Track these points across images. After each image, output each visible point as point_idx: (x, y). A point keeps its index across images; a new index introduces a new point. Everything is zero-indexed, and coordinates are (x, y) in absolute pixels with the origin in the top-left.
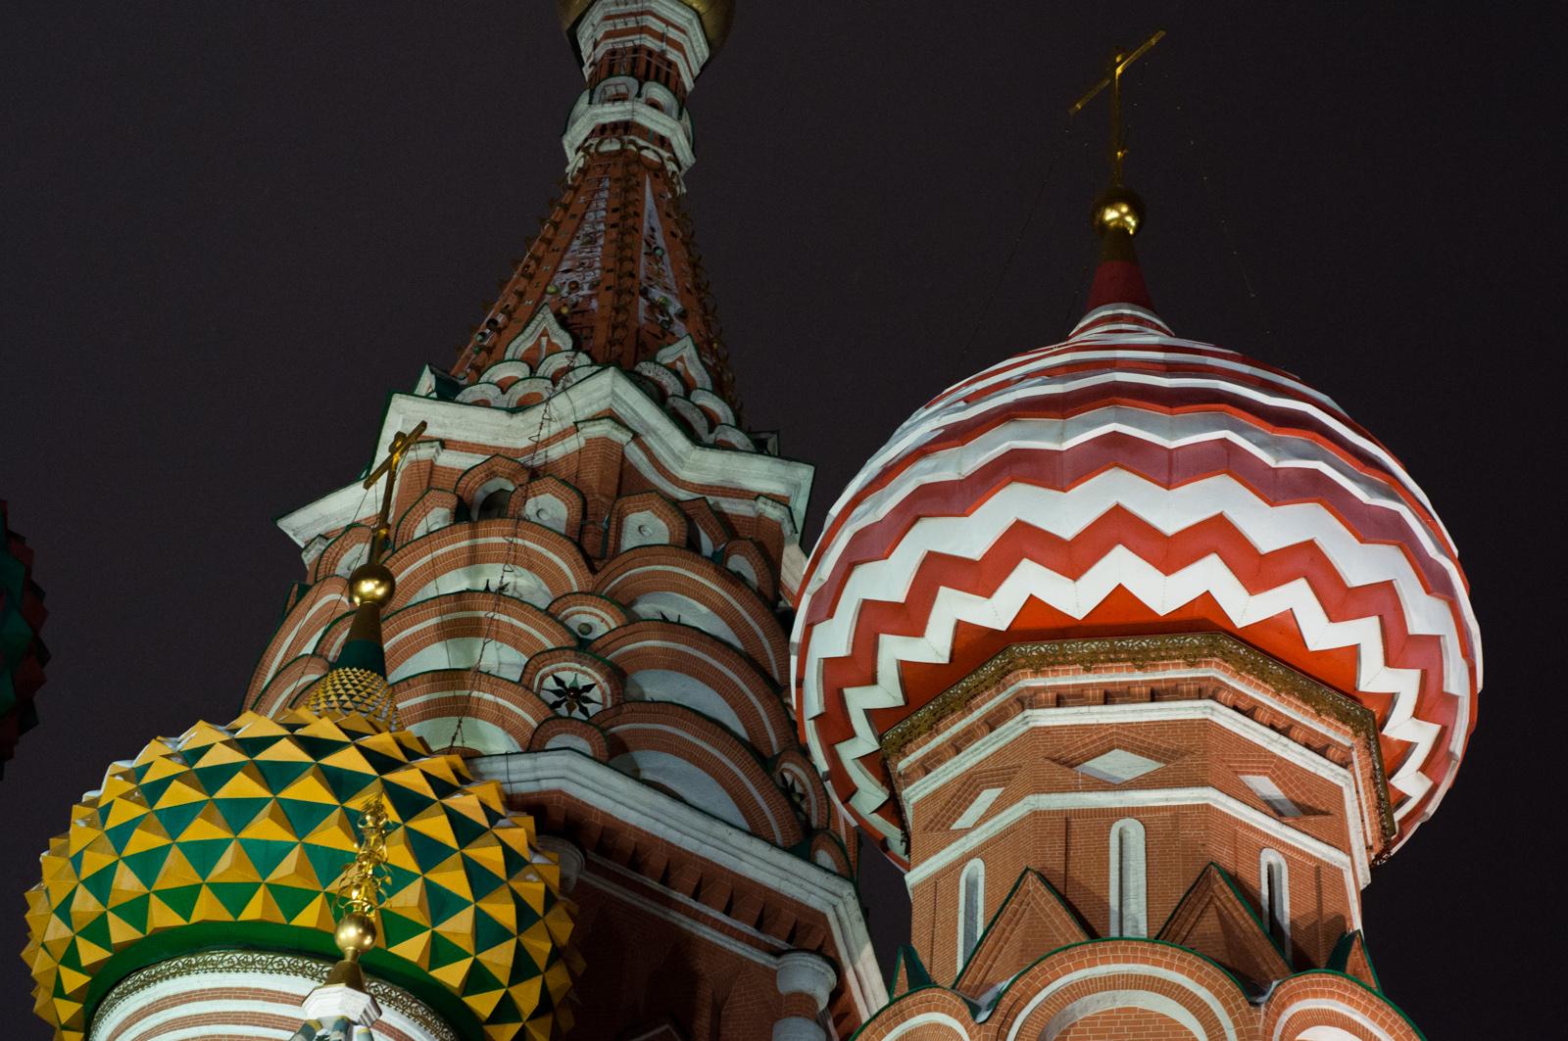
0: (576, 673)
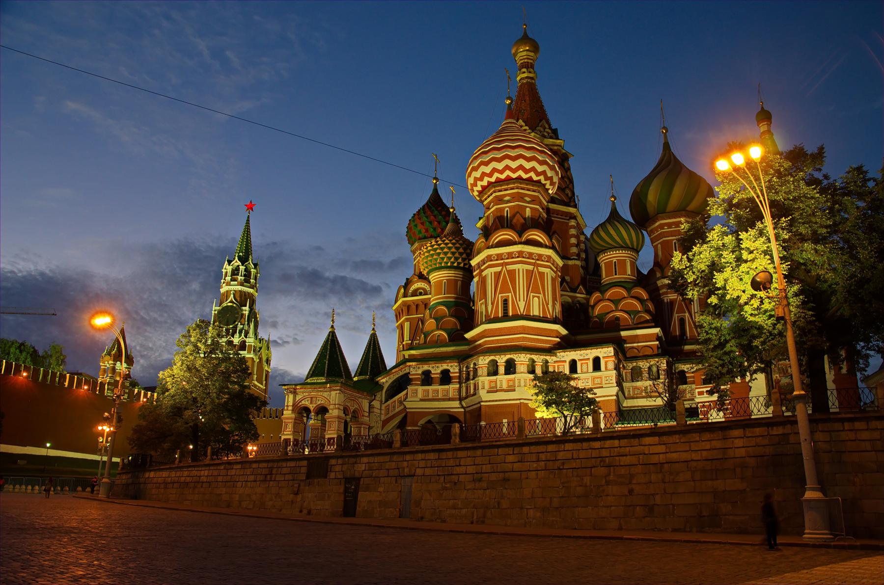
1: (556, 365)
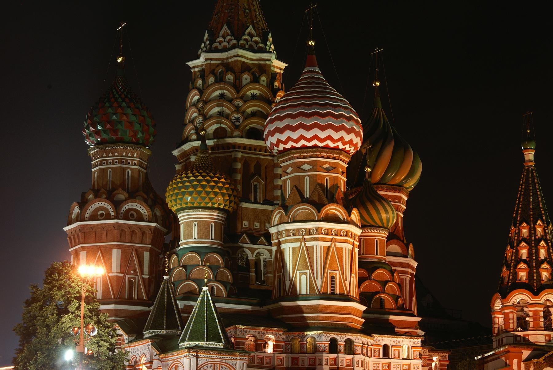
0: (236, 115)
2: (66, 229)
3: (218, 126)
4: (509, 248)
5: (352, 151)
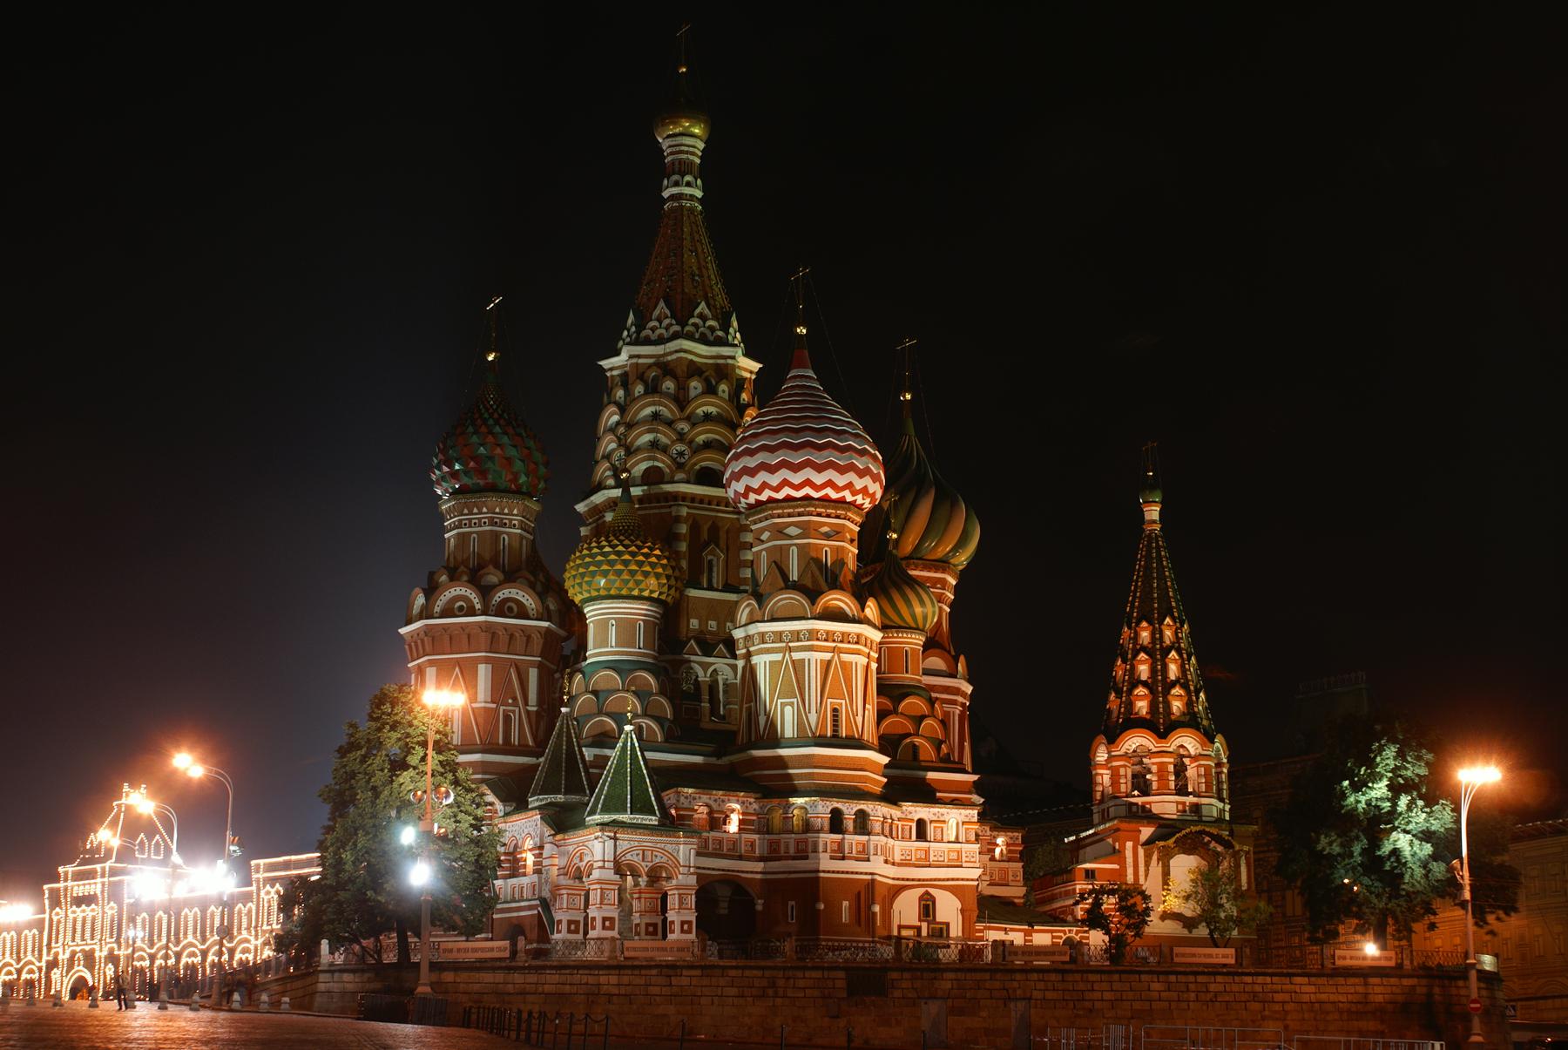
0: (680, 447)
1: (900, 823)
2: (402, 631)
3: (650, 463)
4: (1119, 663)
5: (867, 505)
